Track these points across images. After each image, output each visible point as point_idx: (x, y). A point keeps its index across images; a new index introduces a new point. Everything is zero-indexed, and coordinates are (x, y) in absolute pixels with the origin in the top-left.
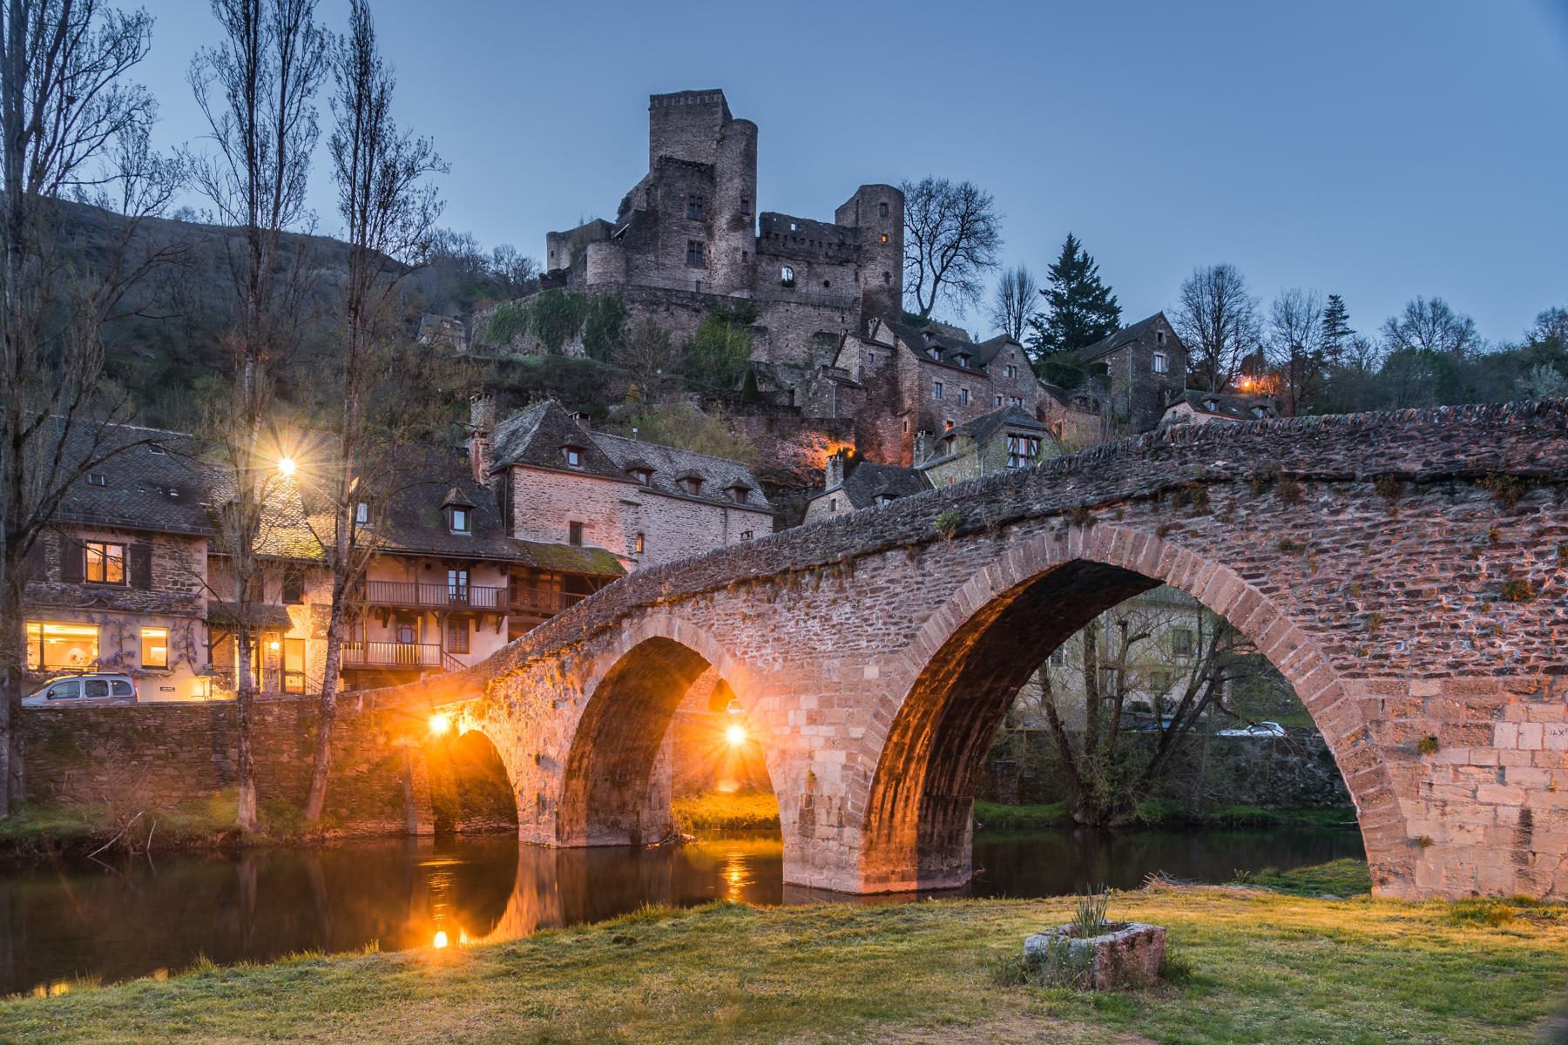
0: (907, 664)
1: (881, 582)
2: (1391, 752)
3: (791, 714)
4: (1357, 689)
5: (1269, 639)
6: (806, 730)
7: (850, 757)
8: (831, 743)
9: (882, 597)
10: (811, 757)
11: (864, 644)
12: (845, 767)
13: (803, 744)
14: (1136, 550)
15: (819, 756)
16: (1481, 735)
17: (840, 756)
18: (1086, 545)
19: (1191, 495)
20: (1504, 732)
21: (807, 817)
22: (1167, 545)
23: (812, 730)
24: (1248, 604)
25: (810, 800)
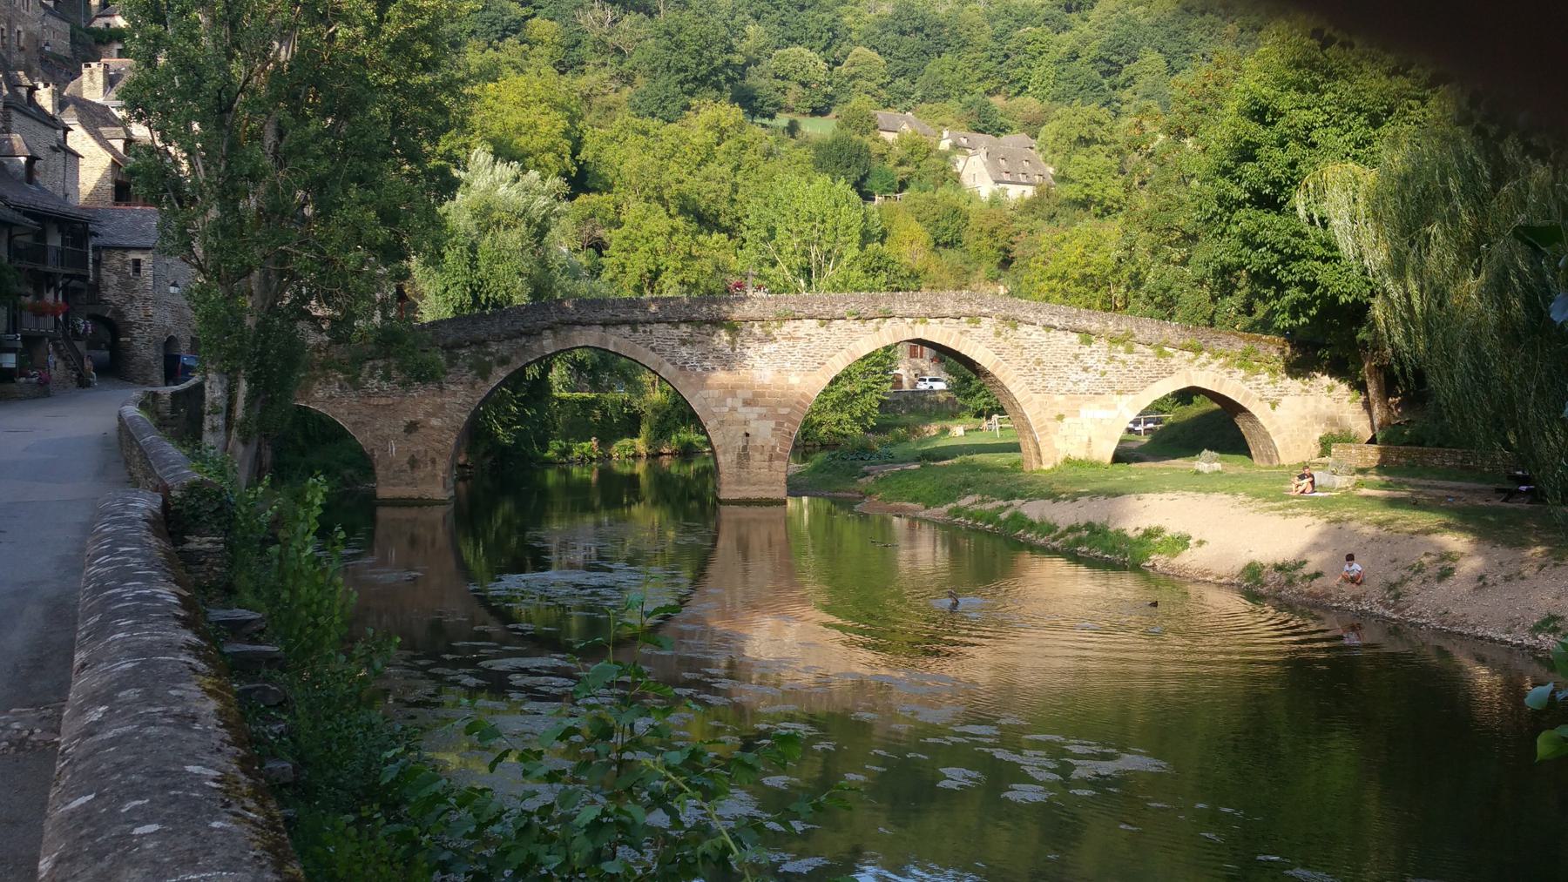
0: (820, 378)
1: (799, 334)
2: (1049, 419)
3: (729, 400)
4: (1037, 398)
5: (1005, 378)
6: (744, 410)
7: (780, 424)
8: (762, 417)
9: (802, 343)
10: (746, 423)
11: (788, 365)
12: (774, 429)
13: (741, 417)
14: (949, 338)
15: (753, 424)
16: (1076, 413)
17: (772, 424)
18: (925, 333)
19: (974, 319)
20: (1083, 411)
21: (744, 456)
22: (964, 338)
23: (748, 409)
24: (997, 365)
25: (745, 448)
